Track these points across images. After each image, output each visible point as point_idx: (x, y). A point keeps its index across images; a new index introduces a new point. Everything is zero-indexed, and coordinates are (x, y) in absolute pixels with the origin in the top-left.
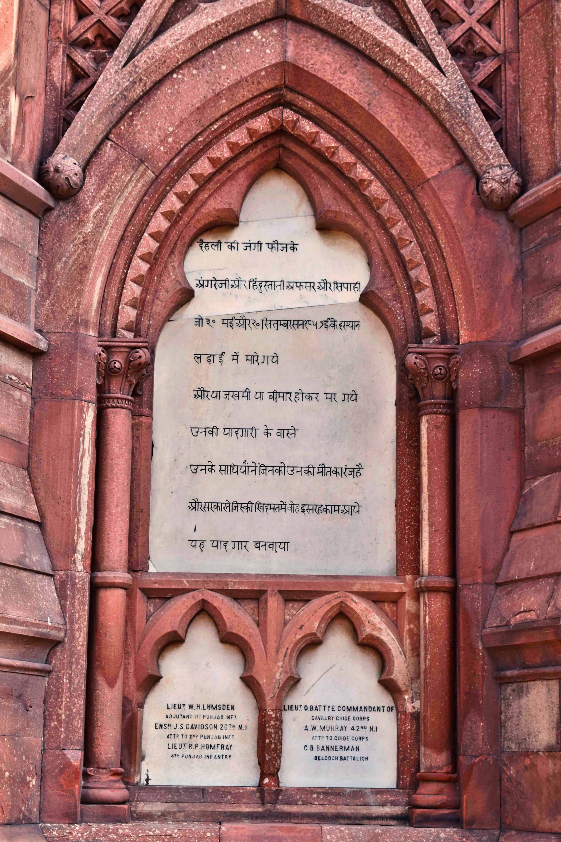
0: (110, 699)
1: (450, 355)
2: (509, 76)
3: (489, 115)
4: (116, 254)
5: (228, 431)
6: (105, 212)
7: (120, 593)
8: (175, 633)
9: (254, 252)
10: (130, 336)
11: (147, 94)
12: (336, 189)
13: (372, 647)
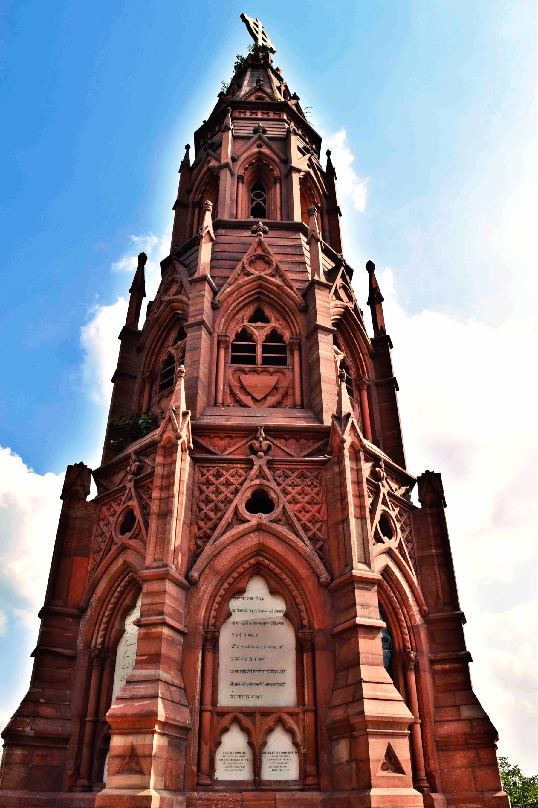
0: (206, 749)
1: (311, 634)
2: (327, 546)
3: (321, 558)
4: (209, 602)
5: (243, 659)
6: (206, 589)
7: (209, 713)
8: (226, 727)
9: (250, 600)
10: (212, 628)
11: (219, 553)
12: (275, 581)
13: (290, 731)
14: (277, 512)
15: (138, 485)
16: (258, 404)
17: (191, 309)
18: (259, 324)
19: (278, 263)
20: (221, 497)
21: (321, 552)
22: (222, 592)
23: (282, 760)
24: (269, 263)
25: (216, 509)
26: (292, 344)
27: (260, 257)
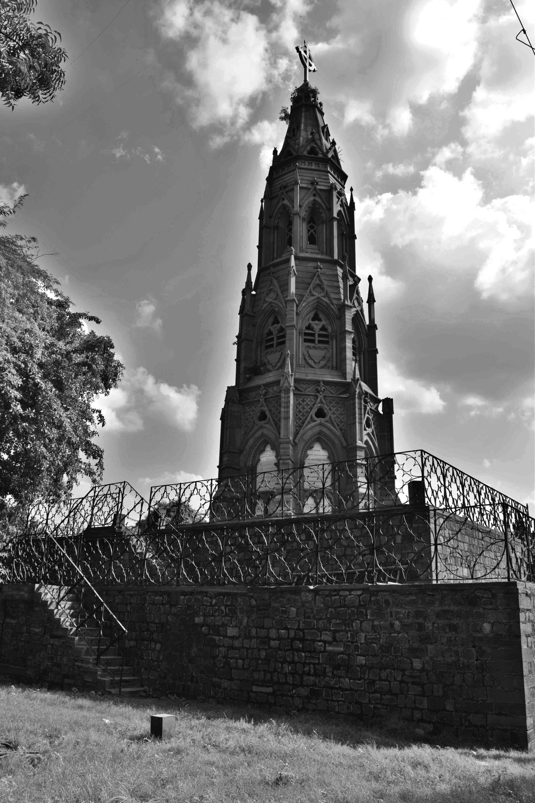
6: (300, 447)
14: (327, 418)
15: (265, 399)
17: (288, 316)
18: (317, 322)
19: (328, 289)
20: (305, 410)
21: (343, 434)
22: (306, 448)
24: (323, 289)
25: (303, 415)
27: (318, 285)
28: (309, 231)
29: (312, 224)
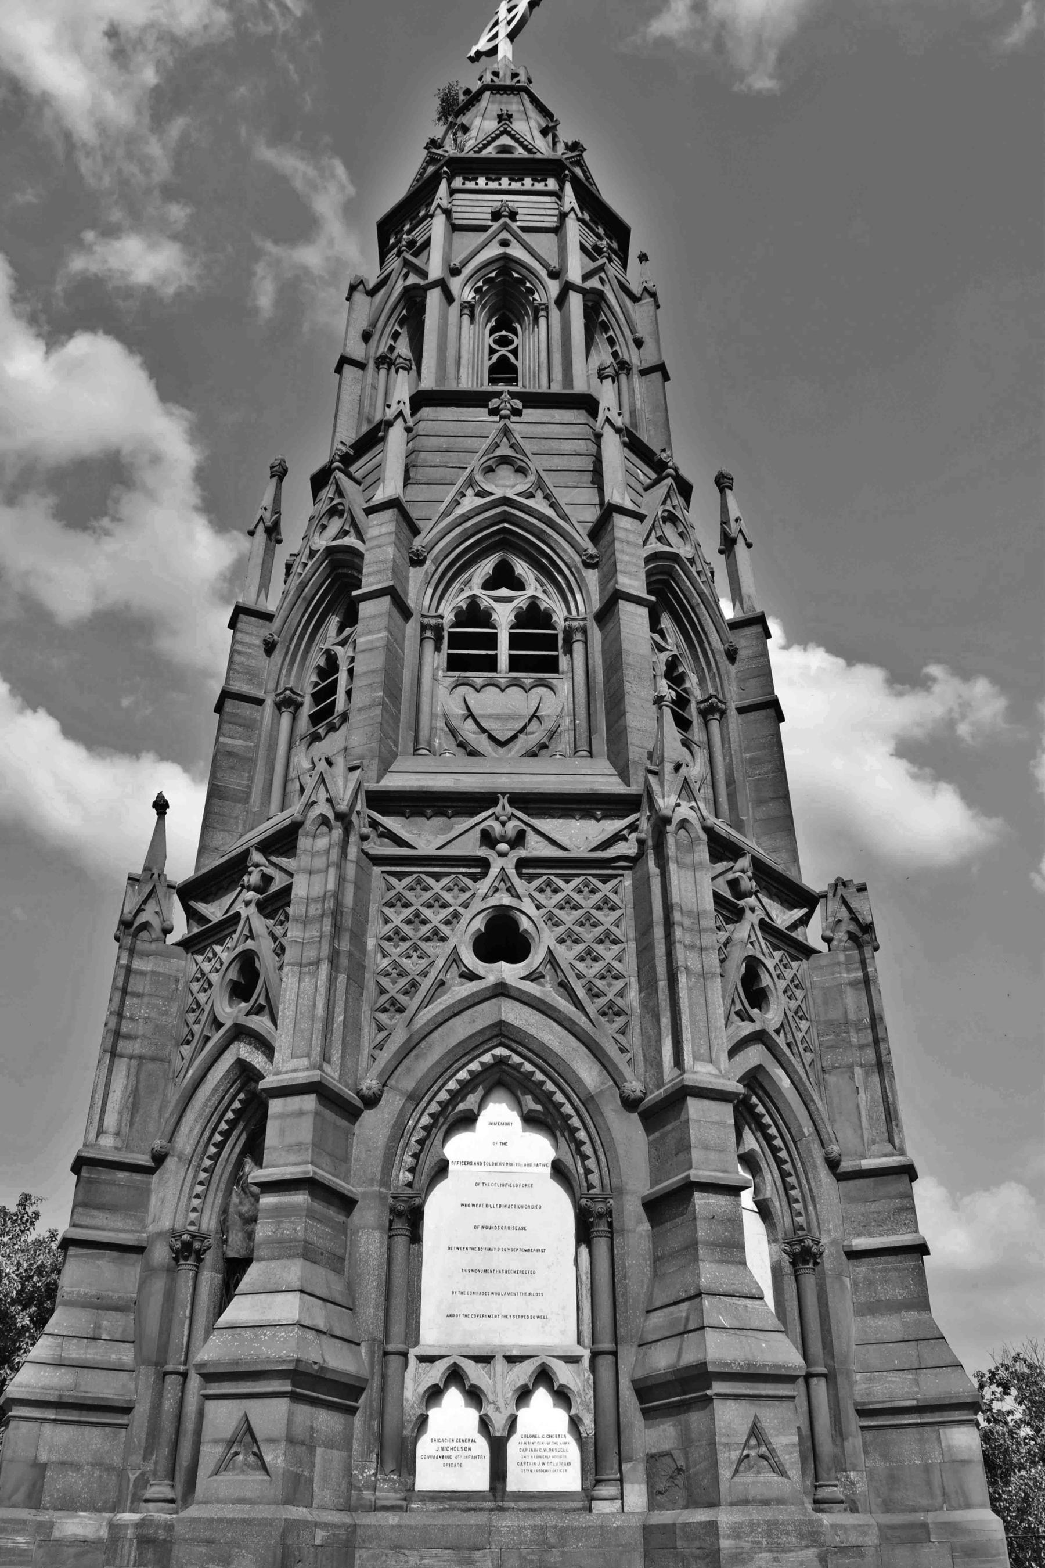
8: (436, 1385)
15: (261, 906)
16: (501, 751)
18: (504, 592)
23: (548, 1451)
26: (569, 632)
27: (504, 460)
28: (492, 351)
29: (504, 333)
